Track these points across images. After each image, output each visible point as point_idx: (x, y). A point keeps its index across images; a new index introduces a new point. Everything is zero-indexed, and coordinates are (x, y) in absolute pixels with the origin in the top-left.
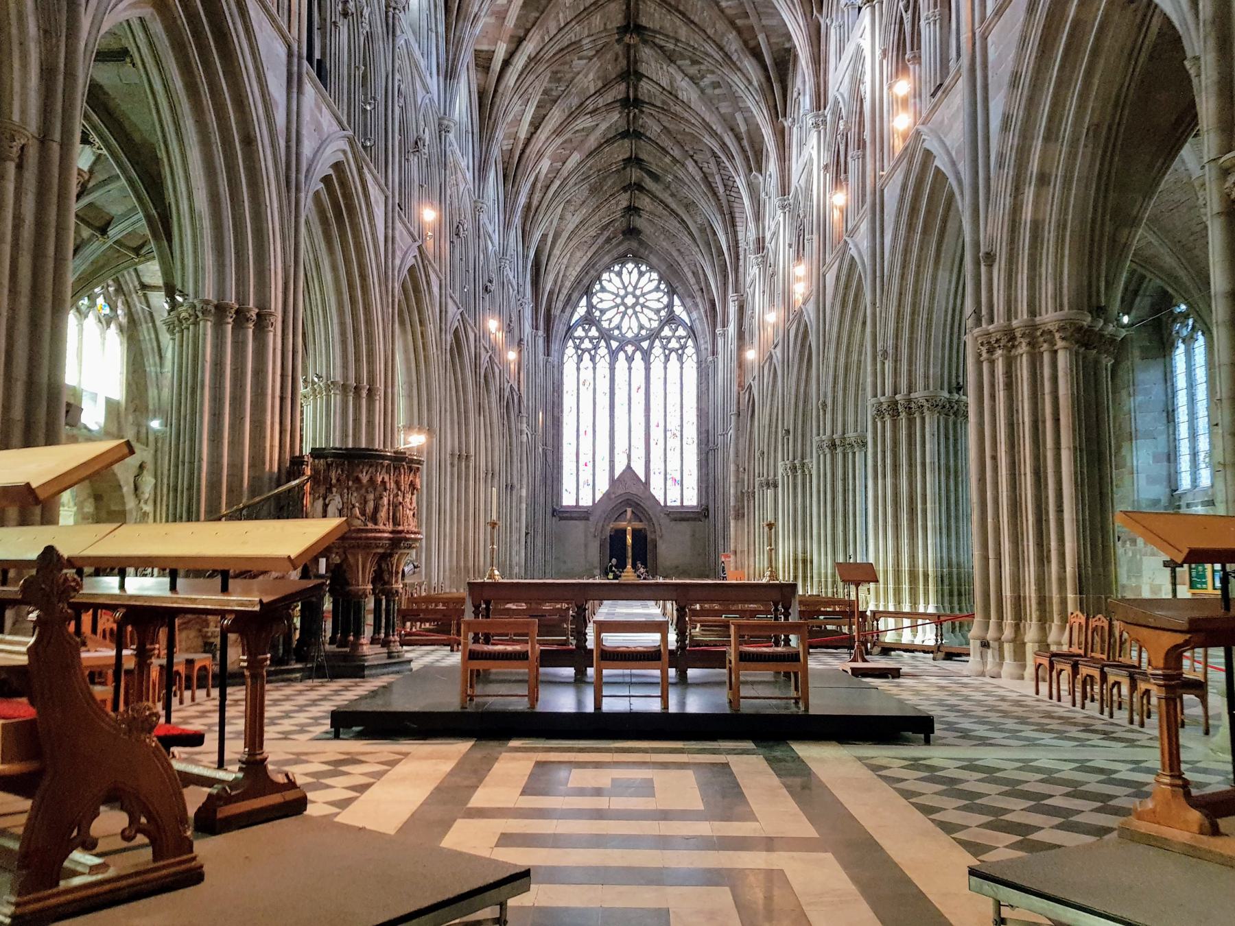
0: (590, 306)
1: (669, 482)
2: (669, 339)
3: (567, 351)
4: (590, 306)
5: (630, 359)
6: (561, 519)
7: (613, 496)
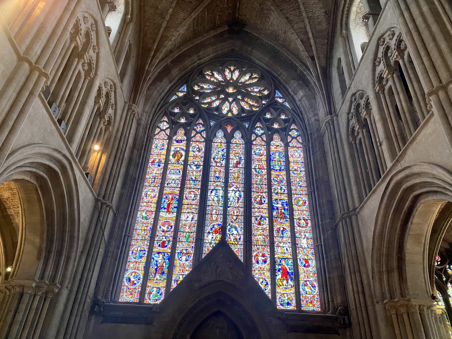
0: (191, 91)
1: (279, 276)
2: (271, 121)
3: (161, 125)
4: (191, 91)
5: (229, 138)
6: (106, 320)
7: (197, 285)
